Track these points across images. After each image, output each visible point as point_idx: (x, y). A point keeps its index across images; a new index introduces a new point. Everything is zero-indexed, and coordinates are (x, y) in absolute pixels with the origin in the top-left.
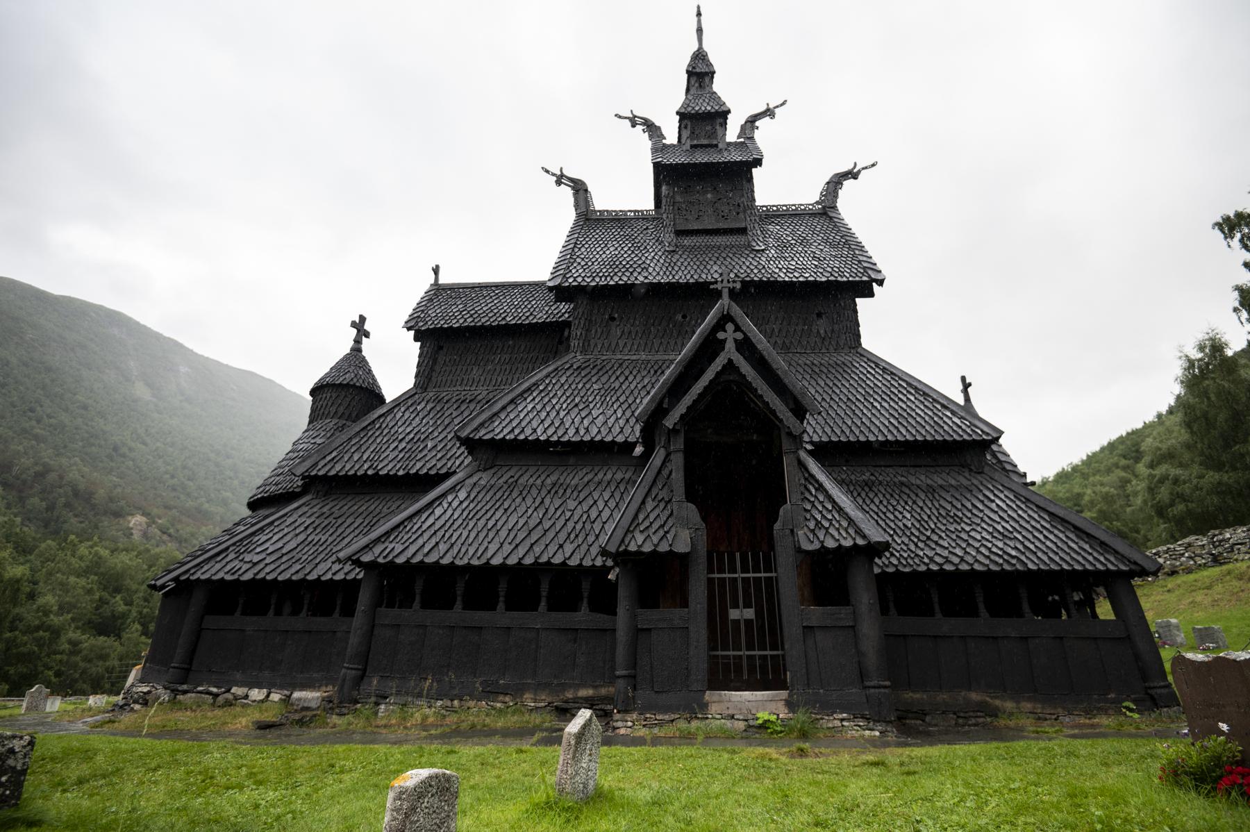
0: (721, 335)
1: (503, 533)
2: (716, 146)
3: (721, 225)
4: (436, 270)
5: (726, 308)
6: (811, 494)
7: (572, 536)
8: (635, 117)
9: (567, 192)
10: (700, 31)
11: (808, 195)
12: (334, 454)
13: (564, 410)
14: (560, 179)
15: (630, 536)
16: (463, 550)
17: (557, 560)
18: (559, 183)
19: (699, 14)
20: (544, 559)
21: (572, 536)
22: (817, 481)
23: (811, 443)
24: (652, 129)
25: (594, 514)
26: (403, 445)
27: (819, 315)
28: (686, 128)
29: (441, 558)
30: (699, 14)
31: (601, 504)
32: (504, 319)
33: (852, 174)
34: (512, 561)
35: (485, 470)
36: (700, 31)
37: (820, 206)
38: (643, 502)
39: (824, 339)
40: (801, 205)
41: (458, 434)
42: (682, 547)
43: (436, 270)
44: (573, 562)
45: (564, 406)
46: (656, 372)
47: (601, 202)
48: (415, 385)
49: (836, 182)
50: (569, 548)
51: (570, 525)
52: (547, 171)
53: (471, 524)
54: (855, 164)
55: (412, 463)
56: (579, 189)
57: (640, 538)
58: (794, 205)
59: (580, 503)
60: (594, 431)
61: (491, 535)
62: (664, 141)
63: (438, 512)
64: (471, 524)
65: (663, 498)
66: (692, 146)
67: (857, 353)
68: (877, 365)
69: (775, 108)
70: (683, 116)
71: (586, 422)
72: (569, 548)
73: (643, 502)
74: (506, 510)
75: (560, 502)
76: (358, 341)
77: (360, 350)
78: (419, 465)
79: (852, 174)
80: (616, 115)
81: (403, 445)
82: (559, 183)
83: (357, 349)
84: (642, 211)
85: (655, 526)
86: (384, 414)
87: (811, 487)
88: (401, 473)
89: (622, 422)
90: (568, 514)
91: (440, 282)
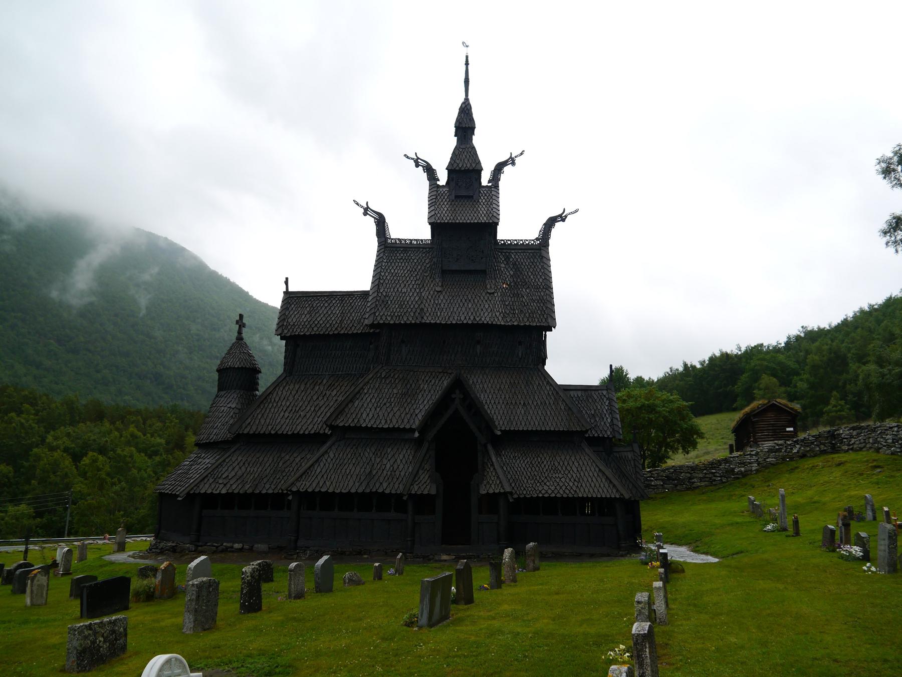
0: (453, 396)
1: (354, 477)
2: (472, 197)
3: (472, 267)
4: (286, 282)
5: (458, 375)
6: (488, 466)
7: (386, 478)
8: (418, 158)
9: (370, 224)
10: (467, 82)
11: (529, 233)
12: (249, 420)
13: (379, 407)
14: (367, 211)
15: (412, 487)
16: (337, 485)
17: (380, 491)
18: (365, 214)
19: (467, 64)
20: (374, 490)
21: (386, 478)
22: (492, 461)
23: (501, 430)
24: (430, 171)
25: (395, 467)
26: (287, 414)
27: (520, 343)
28: (453, 180)
29: (328, 489)
30: (467, 64)
31: (399, 461)
32: (336, 329)
33: (562, 218)
34: (360, 491)
35: (340, 441)
36: (467, 82)
37: (538, 242)
38: (418, 471)
39: (520, 359)
40: (527, 240)
41: (327, 423)
42: (433, 492)
43: (286, 282)
44: (387, 491)
45: (379, 404)
46: (427, 381)
47: (396, 232)
48: (284, 370)
49: (551, 223)
50: (385, 485)
51: (385, 472)
52: (357, 204)
53: (339, 471)
54: (564, 209)
55: (294, 427)
56: (381, 223)
57: (416, 488)
58: (522, 240)
59: (389, 460)
60: (394, 421)
61: (349, 477)
62: (438, 183)
63: (322, 464)
64: (339, 471)
65: (426, 469)
66: (457, 197)
67: (538, 368)
68: (545, 378)
69: (516, 157)
70: (451, 170)
71: (390, 416)
72: (385, 485)
73: (418, 471)
74: (354, 464)
75: (379, 460)
76: (240, 333)
77: (242, 339)
78: (299, 428)
79: (562, 218)
80: (405, 155)
81: (287, 414)
82: (365, 214)
83: (240, 338)
84: (422, 240)
85: (423, 482)
86: (270, 393)
87: (489, 464)
88: (290, 433)
89: (408, 416)
90: (383, 467)
91: (290, 290)
